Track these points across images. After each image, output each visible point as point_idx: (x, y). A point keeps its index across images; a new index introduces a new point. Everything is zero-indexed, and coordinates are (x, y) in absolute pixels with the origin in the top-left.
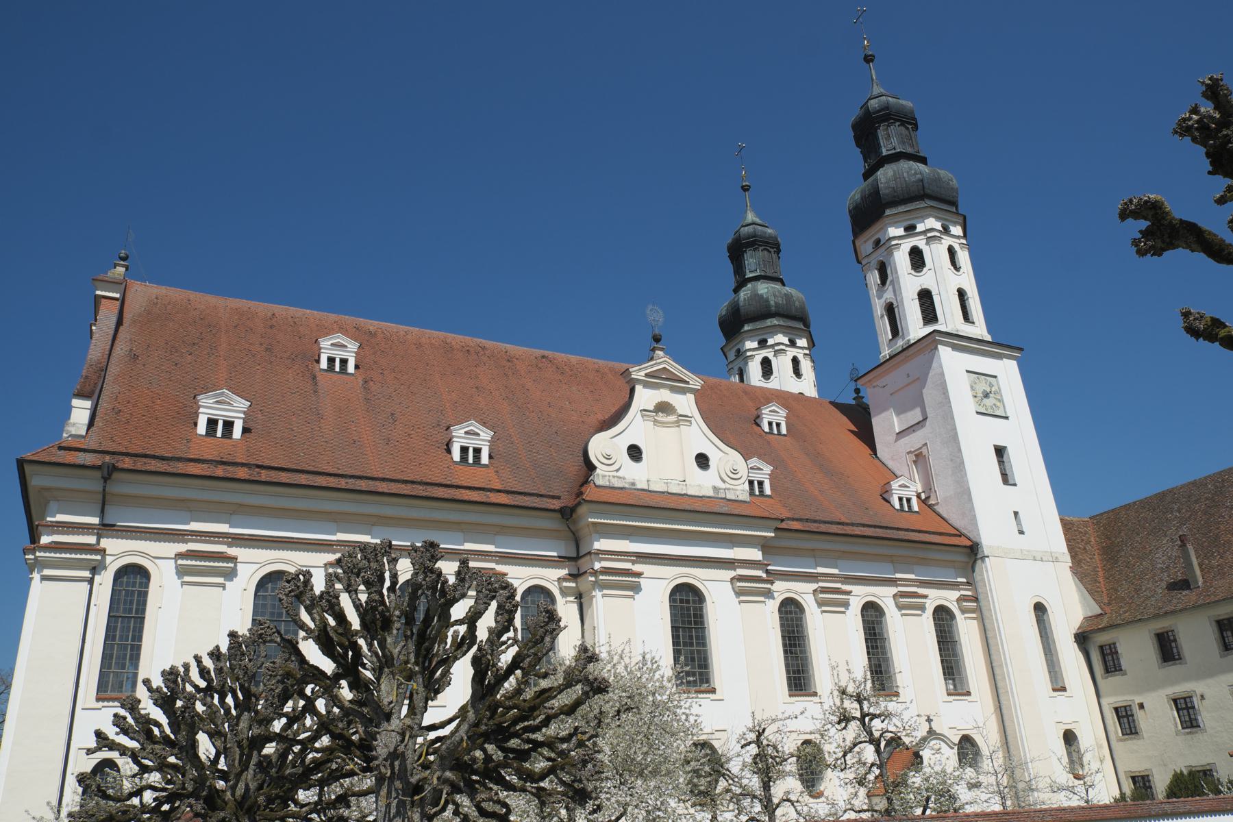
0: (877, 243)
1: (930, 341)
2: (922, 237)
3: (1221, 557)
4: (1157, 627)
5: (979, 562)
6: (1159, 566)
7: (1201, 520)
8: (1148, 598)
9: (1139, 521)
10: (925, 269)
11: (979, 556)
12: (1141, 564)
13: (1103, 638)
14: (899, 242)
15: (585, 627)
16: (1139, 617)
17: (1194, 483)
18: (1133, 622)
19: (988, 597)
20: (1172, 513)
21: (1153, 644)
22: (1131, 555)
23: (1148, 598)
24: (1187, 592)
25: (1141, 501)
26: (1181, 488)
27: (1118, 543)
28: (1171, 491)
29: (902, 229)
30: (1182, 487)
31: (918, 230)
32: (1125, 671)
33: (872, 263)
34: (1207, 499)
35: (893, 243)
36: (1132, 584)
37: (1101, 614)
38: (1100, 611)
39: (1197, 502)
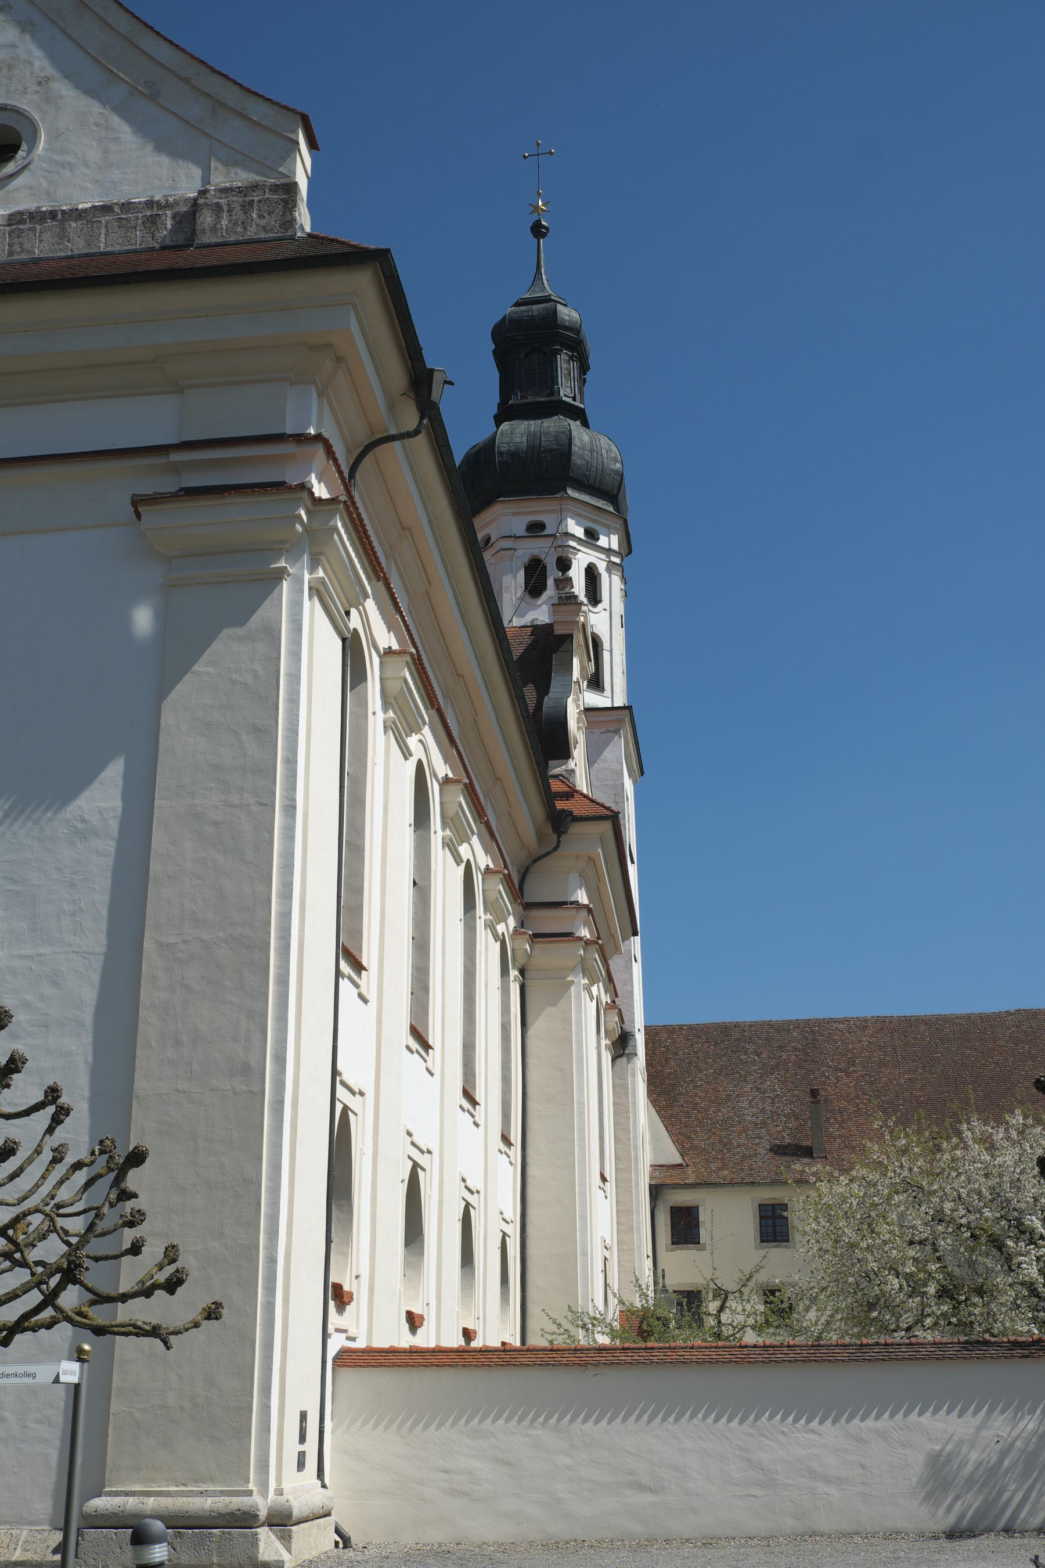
0: (536, 528)
1: (615, 718)
2: (603, 556)
3: (840, 1126)
4: (766, 1196)
5: (624, 1059)
6: (748, 1118)
7: (796, 1074)
8: (744, 1157)
9: (696, 1053)
10: (600, 606)
11: (627, 1052)
12: (719, 1110)
13: (683, 1198)
14: (579, 547)
15: (531, 1032)
16: (748, 1179)
17: (770, 1024)
18: (732, 1184)
19: (628, 1112)
20: (746, 1053)
21: (755, 1217)
22: (696, 1095)
23: (744, 1157)
24: (808, 1160)
25: (691, 1027)
26: (751, 1026)
27: (670, 1074)
28: (737, 1025)
29: (582, 530)
30: (752, 1025)
31: (600, 543)
32: (705, 1244)
33: (519, 553)
34: (796, 1049)
35: (572, 543)
36: (714, 1134)
37: (681, 1165)
38: (678, 1159)
39: (781, 1048)
